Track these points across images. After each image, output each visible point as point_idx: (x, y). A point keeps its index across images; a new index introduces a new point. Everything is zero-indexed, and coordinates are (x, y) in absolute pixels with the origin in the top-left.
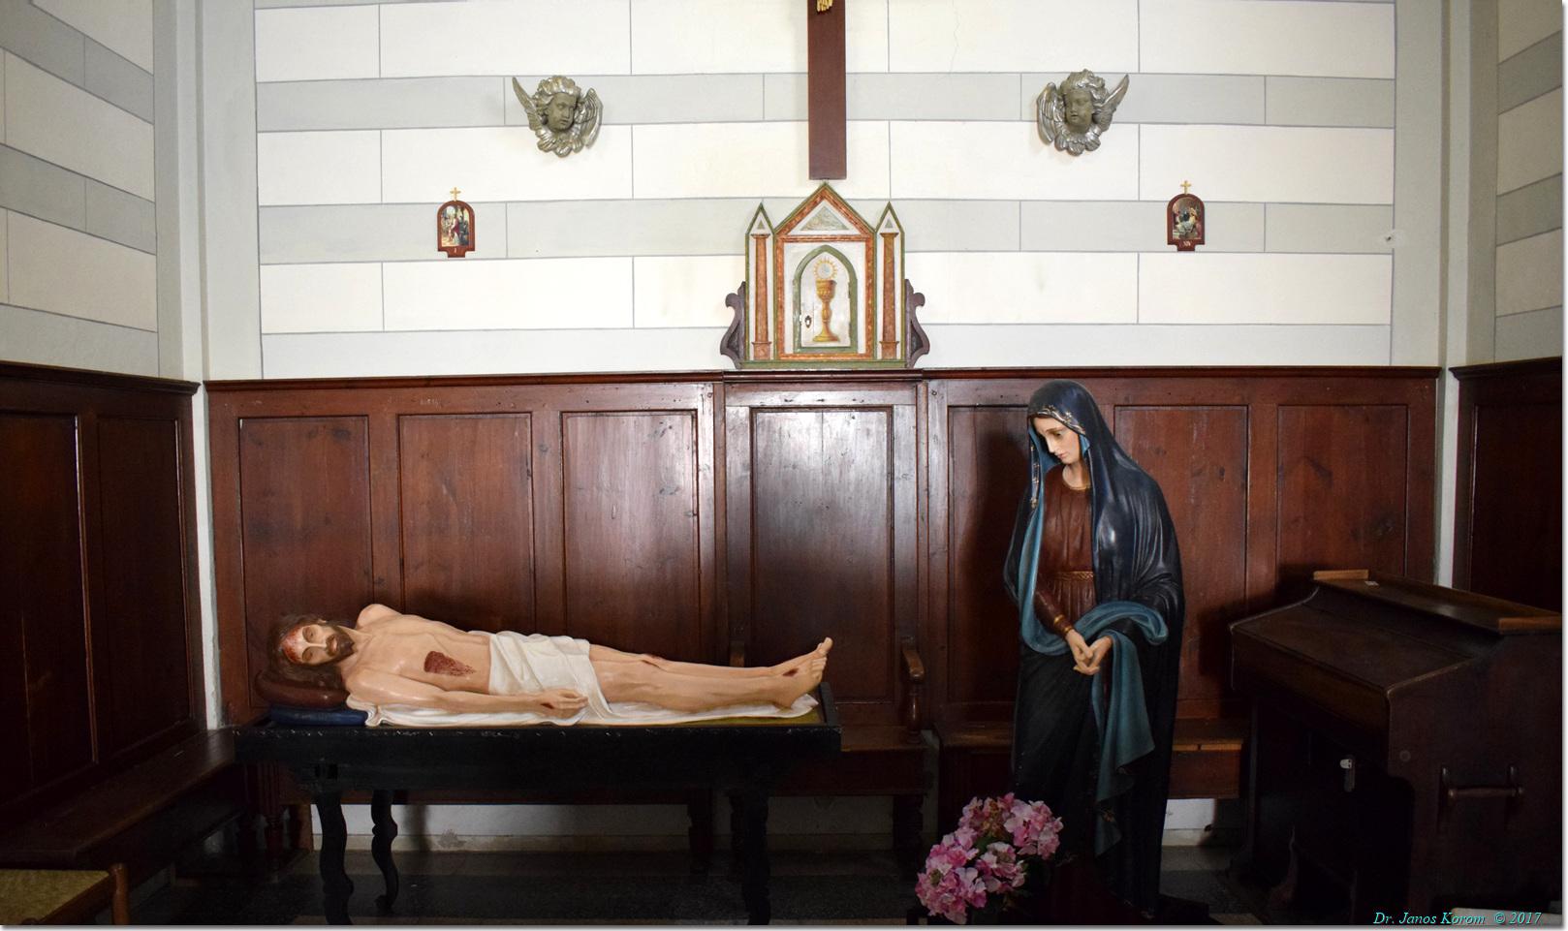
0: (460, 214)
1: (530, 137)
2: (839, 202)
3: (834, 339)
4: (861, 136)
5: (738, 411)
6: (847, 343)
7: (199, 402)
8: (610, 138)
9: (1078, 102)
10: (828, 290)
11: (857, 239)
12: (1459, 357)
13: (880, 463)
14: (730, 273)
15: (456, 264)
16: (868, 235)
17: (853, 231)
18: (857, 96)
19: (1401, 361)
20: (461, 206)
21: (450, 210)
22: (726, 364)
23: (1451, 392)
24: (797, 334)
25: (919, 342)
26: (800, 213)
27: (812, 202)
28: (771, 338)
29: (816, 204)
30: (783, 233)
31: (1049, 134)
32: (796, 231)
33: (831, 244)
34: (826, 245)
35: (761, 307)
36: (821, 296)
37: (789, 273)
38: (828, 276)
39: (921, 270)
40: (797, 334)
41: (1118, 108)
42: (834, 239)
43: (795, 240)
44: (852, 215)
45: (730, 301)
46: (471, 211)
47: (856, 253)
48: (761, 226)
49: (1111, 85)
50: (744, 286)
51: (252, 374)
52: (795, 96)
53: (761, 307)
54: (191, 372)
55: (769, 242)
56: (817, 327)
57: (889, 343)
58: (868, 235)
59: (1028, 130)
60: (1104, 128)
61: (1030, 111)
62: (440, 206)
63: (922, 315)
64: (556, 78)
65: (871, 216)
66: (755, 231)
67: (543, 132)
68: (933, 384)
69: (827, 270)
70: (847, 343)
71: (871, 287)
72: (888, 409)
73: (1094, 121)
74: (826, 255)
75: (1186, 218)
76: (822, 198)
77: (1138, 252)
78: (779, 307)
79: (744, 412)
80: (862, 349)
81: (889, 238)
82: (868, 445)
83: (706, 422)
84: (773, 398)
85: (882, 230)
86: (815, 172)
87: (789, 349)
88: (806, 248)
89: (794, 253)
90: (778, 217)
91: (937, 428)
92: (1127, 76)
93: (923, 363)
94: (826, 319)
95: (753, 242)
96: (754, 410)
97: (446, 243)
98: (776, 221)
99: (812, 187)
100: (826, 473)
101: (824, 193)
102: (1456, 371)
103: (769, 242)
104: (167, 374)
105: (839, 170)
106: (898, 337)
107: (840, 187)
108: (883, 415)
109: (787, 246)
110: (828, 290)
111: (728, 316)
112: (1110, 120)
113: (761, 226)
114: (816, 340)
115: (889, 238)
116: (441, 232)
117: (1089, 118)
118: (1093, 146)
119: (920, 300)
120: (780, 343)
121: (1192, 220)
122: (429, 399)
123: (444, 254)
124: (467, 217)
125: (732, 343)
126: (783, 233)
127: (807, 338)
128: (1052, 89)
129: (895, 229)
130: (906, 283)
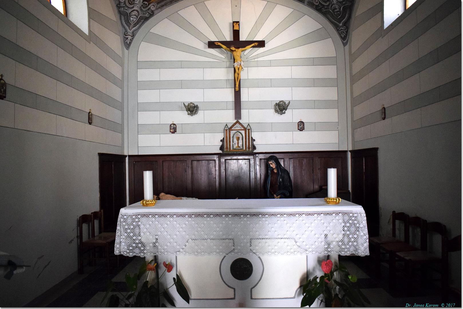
0: (174, 126)
1: (186, 113)
2: (240, 124)
3: (240, 147)
4: (244, 112)
5: (223, 160)
7: (127, 159)
8: (200, 112)
9: (281, 106)
10: (238, 139)
11: (243, 130)
12: (350, 149)
13: (248, 169)
14: (221, 136)
15: (173, 135)
16: (245, 129)
17: (243, 128)
18: (243, 105)
19: (340, 150)
20: (174, 124)
21: (172, 125)
22: (221, 152)
23: (349, 155)
24: (233, 146)
25: (254, 148)
27: (235, 124)
28: (228, 147)
29: (236, 124)
30: (230, 129)
31: (276, 111)
32: (233, 129)
33: (239, 131)
34: (238, 131)
35: (227, 142)
36: (237, 140)
37: (231, 136)
38: (238, 136)
39: (254, 135)
40: (233, 146)
41: (288, 107)
42: (239, 130)
43: (232, 130)
44: (242, 126)
45: (221, 141)
46: (176, 125)
47: (243, 132)
48: (226, 128)
49: (287, 103)
50: (224, 138)
51: (137, 154)
52: (232, 105)
53: (227, 142)
54: (126, 153)
55: (228, 131)
56: (236, 145)
57: (249, 148)
58: (245, 129)
59: (273, 111)
60: (286, 110)
61: (273, 107)
62: (170, 125)
63: (255, 143)
64: (191, 103)
65: (245, 126)
66: (225, 129)
67: (188, 112)
68: (257, 155)
69: (238, 135)
70: (242, 148)
72: (249, 159)
73: (284, 109)
74: (238, 133)
75: (301, 125)
76: (237, 123)
78: (230, 142)
79: (224, 160)
80: (244, 149)
81: (249, 130)
82: (246, 166)
83: (217, 162)
84: (229, 158)
85: (247, 128)
86: (236, 118)
88: (234, 131)
89: (232, 132)
90: (229, 126)
91: (258, 163)
92: (289, 102)
93: (255, 151)
94: (238, 144)
95: (225, 131)
96: (225, 160)
97: (171, 131)
99: (235, 121)
100: (238, 170)
101: (238, 122)
102: (350, 151)
103: (228, 131)
104: (123, 154)
105: (240, 118)
106: (251, 147)
107: (241, 121)
108: (248, 160)
109: (231, 131)
110: (238, 139)
111: (221, 143)
112: (287, 109)
113: (226, 128)
114: (236, 147)
115: (249, 130)
116: (170, 129)
117: (283, 109)
118: (285, 113)
119: (254, 140)
120: (230, 148)
121: (302, 126)
122: (168, 158)
123: (171, 133)
124: (175, 126)
125: (222, 148)
126: (230, 129)
127: (235, 147)
128: (276, 104)
129: (250, 128)
130: (252, 137)
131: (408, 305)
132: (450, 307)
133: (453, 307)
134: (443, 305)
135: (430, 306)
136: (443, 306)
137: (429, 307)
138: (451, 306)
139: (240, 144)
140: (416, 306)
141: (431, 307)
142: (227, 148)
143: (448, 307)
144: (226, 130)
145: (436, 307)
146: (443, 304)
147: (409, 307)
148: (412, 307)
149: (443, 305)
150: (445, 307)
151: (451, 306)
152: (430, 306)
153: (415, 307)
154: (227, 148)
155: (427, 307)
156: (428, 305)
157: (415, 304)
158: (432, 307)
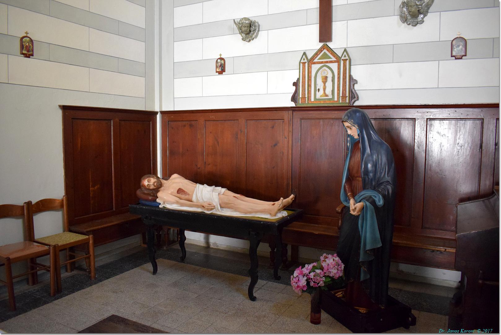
0: (221, 61)
1: (239, 37)
3: (327, 96)
4: (337, 27)
6: (330, 97)
8: (262, 34)
9: (411, 6)
10: (325, 79)
11: (334, 62)
14: (294, 75)
15: (221, 76)
16: (338, 60)
17: (334, 59)
18: (336, 13)
20: (221, 59)
21: (219, 60)
22: (293, 104)
25: (354, 96)
26: (316, 54)
27: (320, 50)
28: (306, 96)
29: (322, 51)
30: (311, 61)
31: (404, 19)
32: (316, 60)
33: (327, 64)
36: (323, 82)
38: (325, 75)
39: (357, 72)
41: (431, 8)
42: (327, 62)
43: (315, 63)
45: (295, 84)
46: (224, 60)
47: (334, 66)
48: (304, 59)
50: (298, 79)
52: (315, 16)
55: (306, 64)
56: (322, 92)
57: (344, 97)
59: (396, 19)
60: (425, 16)
61: (397, 12)
62: (217, 59)
66: (302, 61)
67: (243, 35)
69: (325, 73)
70: (330, 97)
71: (339, 78)
73: (419, 12)
74: (325, 68)
75: (459, 46)
76: (324, 49)
77: (439, 61)
80: (336, 99)
81: (345, 60)
85: (343, 58)
87: (313, 99)
88: (319, 66)
89: (315, 68)
90: (310, 56)
95: (301, 64)
97: (218, 70)
98: (309, 57)
103: (306, 64)
105: (330, 39)
106: (347, 95)
107: (331, 45)
109: (313, 65)
110: (325, 79)
112: (427, 12)
113: (304, 59)
114: (321, 96)
115: (345, 60)
116: (217, 67)
117: (417, 12)
118: (422, 22)
119: (356, 82)
120: (309, 97)
121: (461, 47)
123: (218, 73)
124: (223, 63)
125: (294, 99)
126: (311, 61)
129: (347, 58)
135: (465, 332)
139: (329, 91)
141: (466, 333)
142: (304, 98)
144: (304, 63)
152: (465, 332)
154: (304, 98)
156: (463, 331)
158: (468, 333)
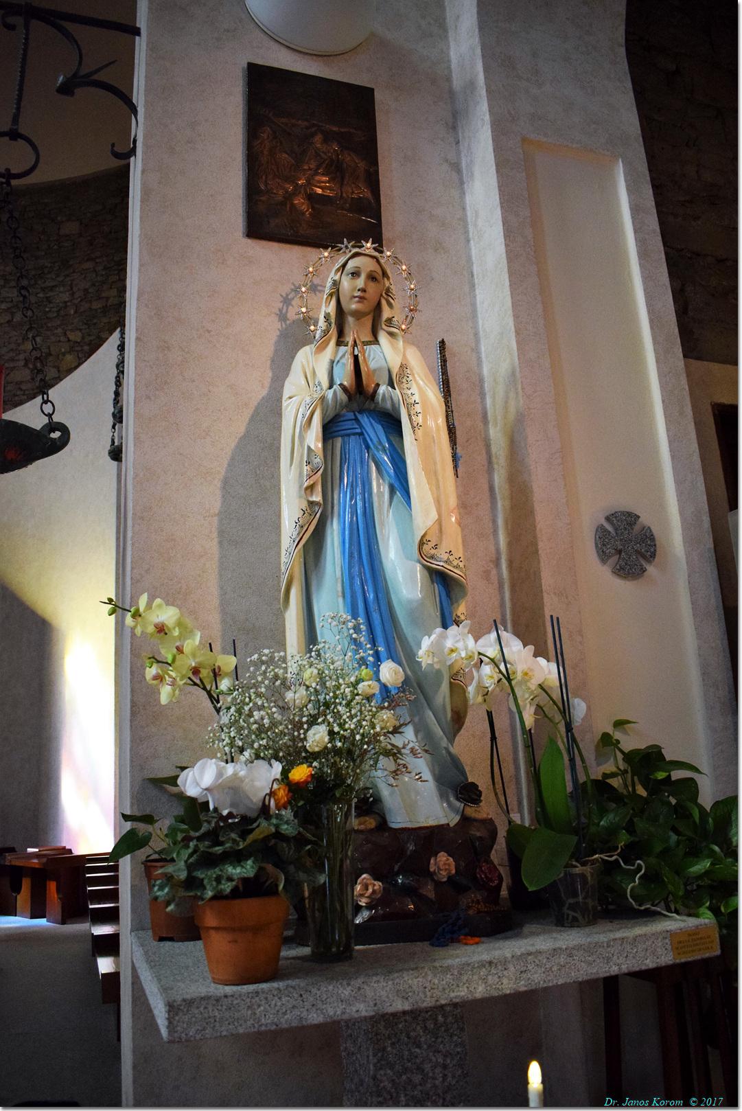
131: (609, 1101)
132: (711, 1106)
133: (717, 1106)
134: (694, 1102)
135: (662, 1103)
136: (694, 1104)
137: (660, 1106)
138: (713, 1103)
140: (630, 1103)
141: (664, 1106)
143: (706, 1106)
145: (677, 1106)
146: (694, 1099)
147: (611, 1106)
148: (621, 1106)
149: (694, 1102)
150: (698, 1106)
151: (713, 1103)
152: (662, 1103)
153: (627, 1106)
155: (655, 1106)
156: (658, 1102)
157: (627, 1099)
158: (668, 1106)
